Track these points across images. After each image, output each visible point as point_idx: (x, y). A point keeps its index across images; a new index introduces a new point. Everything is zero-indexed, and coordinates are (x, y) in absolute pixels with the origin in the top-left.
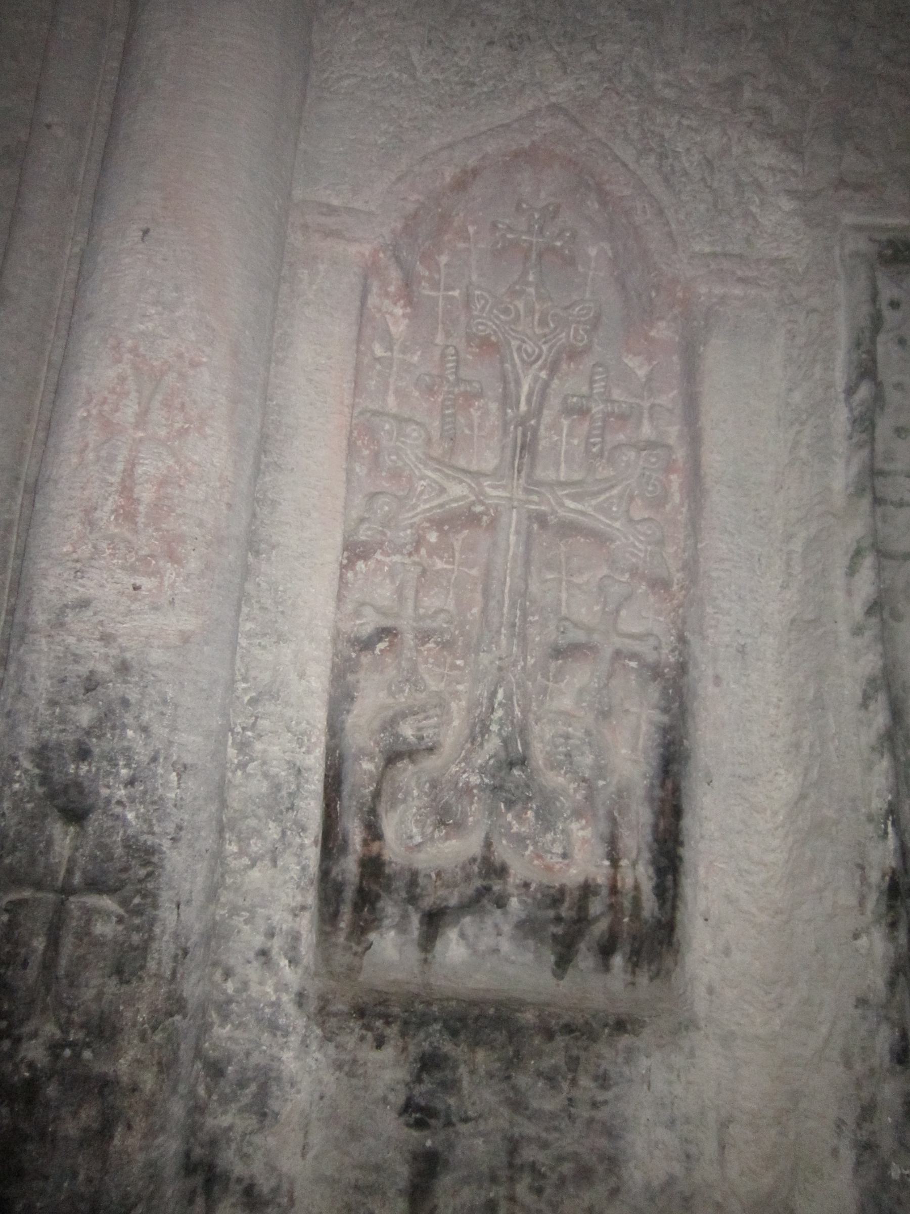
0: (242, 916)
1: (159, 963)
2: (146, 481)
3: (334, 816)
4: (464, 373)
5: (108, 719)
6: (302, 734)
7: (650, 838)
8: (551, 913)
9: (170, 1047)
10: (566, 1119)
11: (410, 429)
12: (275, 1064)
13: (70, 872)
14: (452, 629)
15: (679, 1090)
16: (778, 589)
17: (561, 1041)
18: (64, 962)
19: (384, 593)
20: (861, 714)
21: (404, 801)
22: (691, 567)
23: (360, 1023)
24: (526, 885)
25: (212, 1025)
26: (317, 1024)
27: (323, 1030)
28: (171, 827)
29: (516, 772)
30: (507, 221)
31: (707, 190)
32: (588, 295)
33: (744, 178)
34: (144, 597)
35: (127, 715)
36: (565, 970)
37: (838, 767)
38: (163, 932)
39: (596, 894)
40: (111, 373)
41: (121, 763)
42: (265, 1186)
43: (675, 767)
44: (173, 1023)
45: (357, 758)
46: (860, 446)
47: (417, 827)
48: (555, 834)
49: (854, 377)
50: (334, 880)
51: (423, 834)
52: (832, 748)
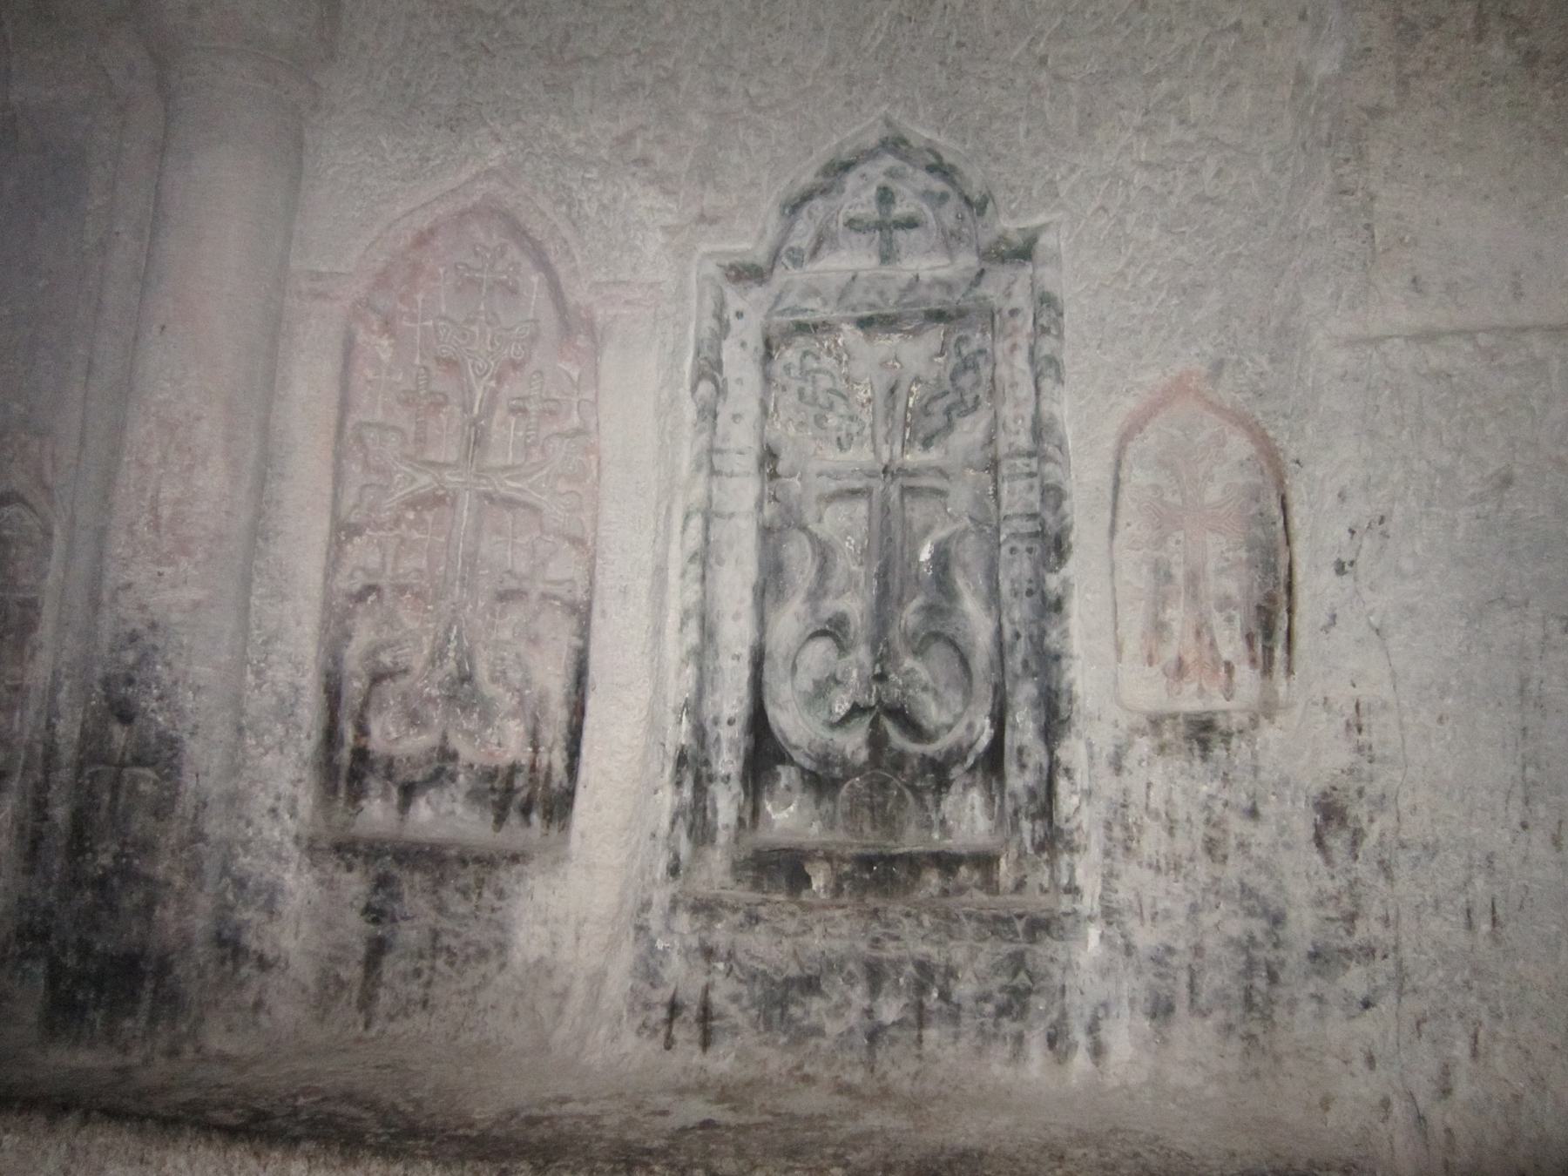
5: (144, 659)
7: (565, 731)
17: (472, 867)
19: (373, 560)
24: (471, 766)
25: (237, 856)
28: (188, 726)
42: (270, 955)
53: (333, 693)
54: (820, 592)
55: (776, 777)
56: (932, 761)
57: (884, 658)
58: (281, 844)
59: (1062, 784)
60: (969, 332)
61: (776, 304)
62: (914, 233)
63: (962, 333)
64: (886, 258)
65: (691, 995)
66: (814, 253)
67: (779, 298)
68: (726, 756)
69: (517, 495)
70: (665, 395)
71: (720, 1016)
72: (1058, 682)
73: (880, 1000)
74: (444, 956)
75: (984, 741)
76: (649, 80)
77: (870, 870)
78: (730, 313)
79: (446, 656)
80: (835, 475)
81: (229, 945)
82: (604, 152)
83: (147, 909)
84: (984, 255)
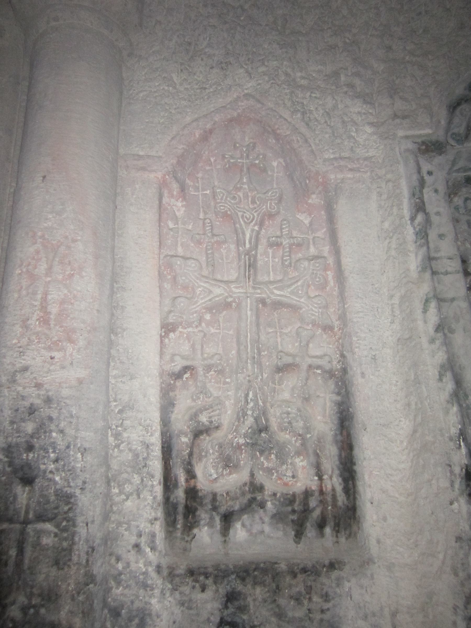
0: (124, 527)
1: (79, 555)
2: (54, 303)
3: (169, 468)
4: (215, 231)
5: (42, 428)
6: (147, 426)
7: (337, 463)
8: (290, 509)
9: (88, 603)
10: (308, 621)
11: (190, 262)
12: (148, 606)
13: (27, 512)
14: (222, 363)
15: (367, 598)
16: (389, 324)
17: (301, 577)
18: (26, 561)
19: (185, 348)
20: (440, 384)
21: (206, 456)
22: (343, 317)
23: (192, 579)
24: (275, 495)
25: (112, 588)
26: (168, 582)
27: (172, 585)
28: (80, 483)
29: (263, 435)
30: (230, 154)
31: (328, 127)
32: (275, 186)
33: (346, 119)
34: (58, 362)
35: (52, 425)
36: (300, 538)
37: (431, 414)
38: (80, 540)
39: (312, 495)
40: (32, 250)
41: (51, 451)
43: (347, 423)
44: (89, 589)
45: (178, 436)
46: (421, 246)
47: (213, 469)
48: (287, 465)
49: (414, 211)
50: (172, 503)
51: (217, 473)
52: (427, 404)
58: (145, 573)
76: (340, 44)
79: (247, 415)
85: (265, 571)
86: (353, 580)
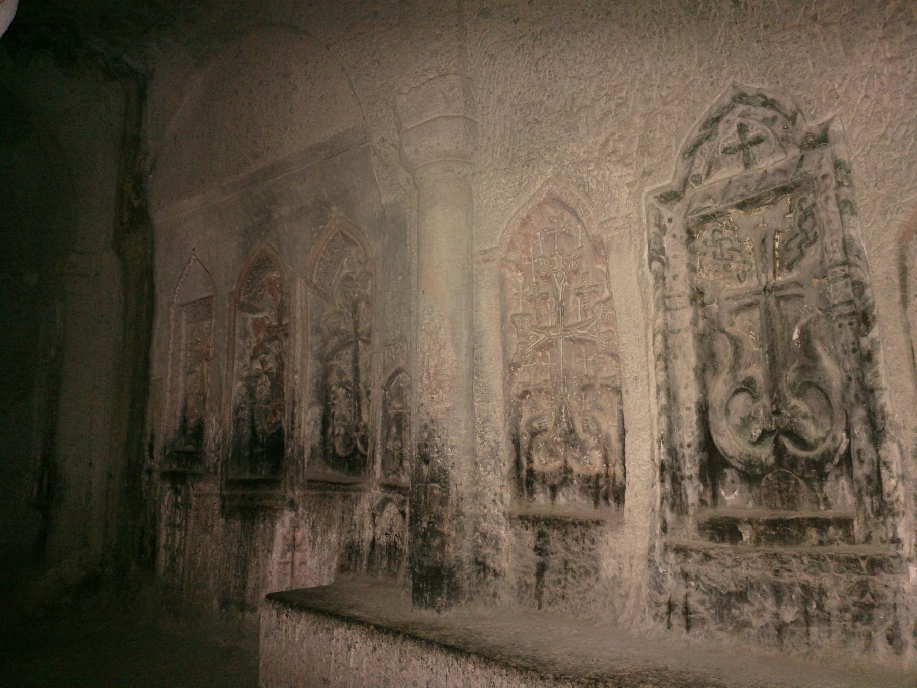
5: (430, 436)
19: (527, 378)
28: (451, 464)
42: (498, 569)
53: (516, 442)
54: (737, 366)
55: (725, 475)
56: (813, 461)
57: (777, 400)
58: (498, 516)
59: (884, 473)
60: (806, 195)
61: (688, 209)
62: (762, 145)
63: (802, 196)
64: (747, 165)
65: (679, 599)
66: (708, 175)
67: (689, 206)
68: (689, 465)
69: (582, 337)
70: (640, 273)
71: (695, 612)
72: (874, 406)
73: (783, 607)
74: (570, 573)
75: (844, 447)
77: (775, 530)
78: (665, 221)
80: (736, 298)
81: (481, 565)
82: (596, 154)
83: (442, 545)
84: (801, 147)
85: (560, 521)
86: (610, 533)
